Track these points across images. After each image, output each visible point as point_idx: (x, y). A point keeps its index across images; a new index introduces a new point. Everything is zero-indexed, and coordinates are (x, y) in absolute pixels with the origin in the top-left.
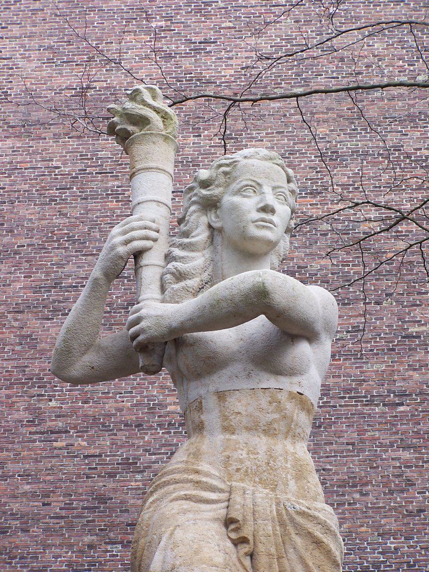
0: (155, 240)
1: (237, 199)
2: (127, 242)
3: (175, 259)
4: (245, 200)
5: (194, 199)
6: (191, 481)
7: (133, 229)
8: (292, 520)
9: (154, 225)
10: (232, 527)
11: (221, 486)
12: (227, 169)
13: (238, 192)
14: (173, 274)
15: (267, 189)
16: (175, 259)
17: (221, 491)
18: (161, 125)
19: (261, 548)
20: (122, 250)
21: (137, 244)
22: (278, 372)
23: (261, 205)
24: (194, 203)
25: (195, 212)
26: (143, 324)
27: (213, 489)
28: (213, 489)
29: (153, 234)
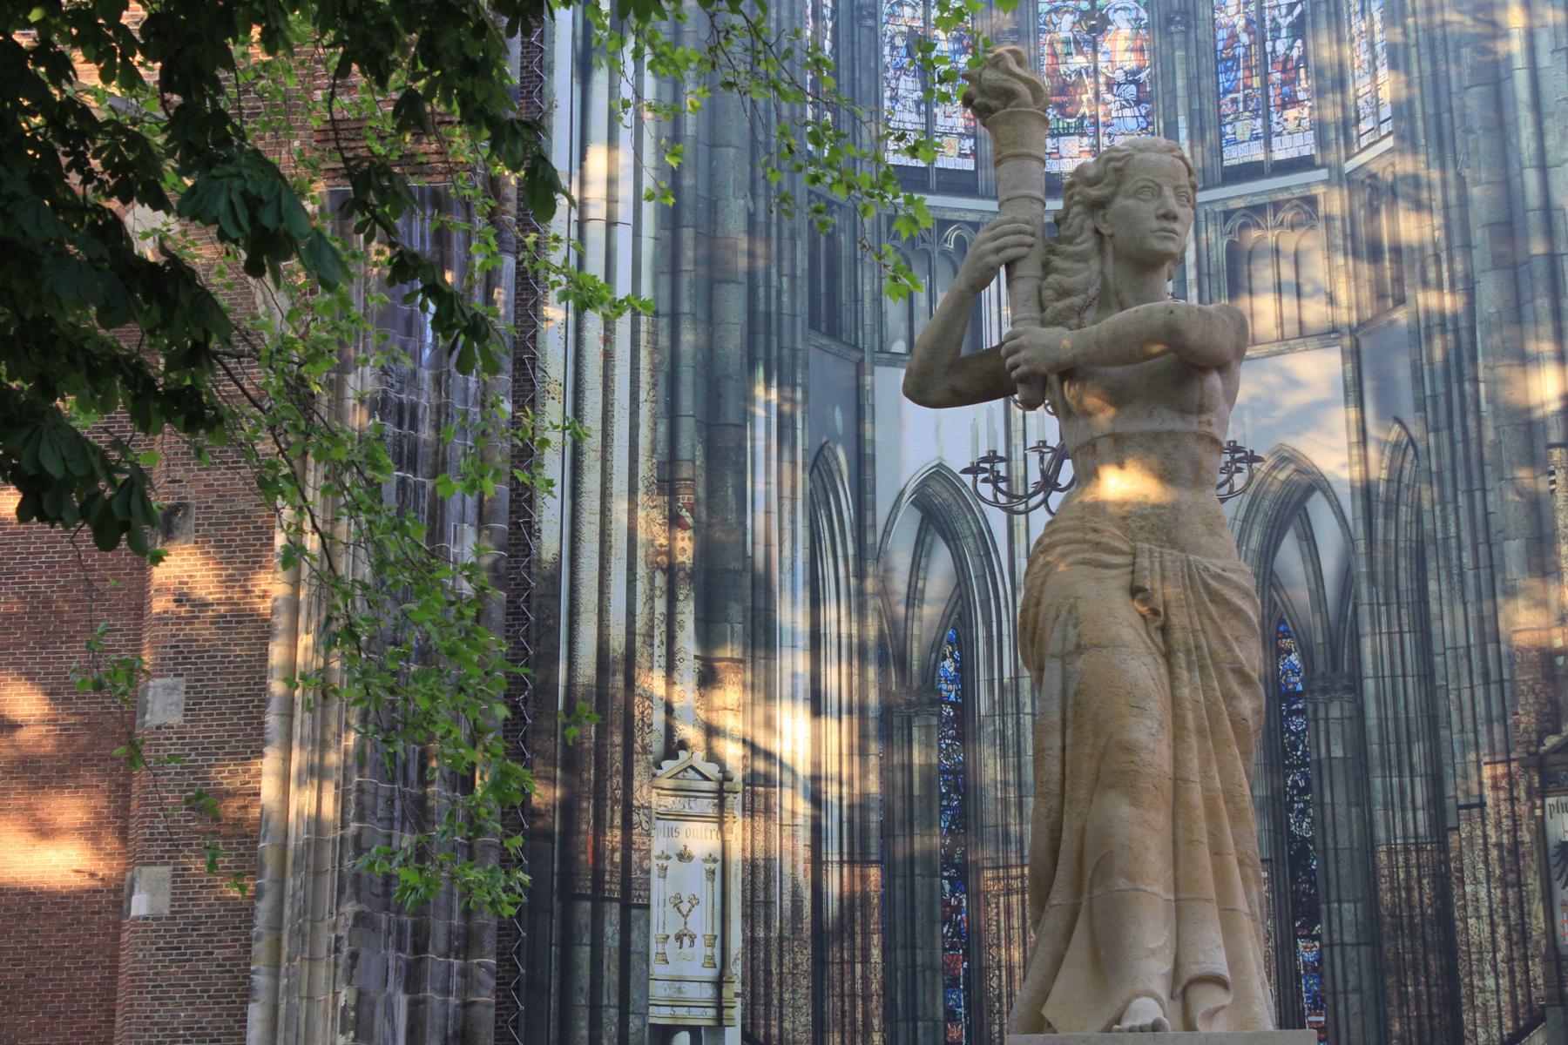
0: (1030, 246)
1: (1130, 202)
2: (998, 250)
3: (1056, 271)
4: (1143, 205)
5: (1077, 198)
6: (1089, 542)
7: (1005, 235)
8: (1206, 586)
9: (1028, 228)
10: (1140, 596)
11: (1125, 548)
12: (1118, 164)
13: (1135, 194)
14: (1055, 290)
15: (1168, 191)
16: (1056, 271)
17: (1123, 553)
18: (1030, 99)
19: (1174, 620)
20: (992, 259)
21: (1010, 253)
22: (1184, 411)
23: (1162, 212)
24: (1078, 203)
25: (1078, 214)
26: (1022, 355)
27: (1115, 551)
28: (1115, 551)
29: (1029, 239)
